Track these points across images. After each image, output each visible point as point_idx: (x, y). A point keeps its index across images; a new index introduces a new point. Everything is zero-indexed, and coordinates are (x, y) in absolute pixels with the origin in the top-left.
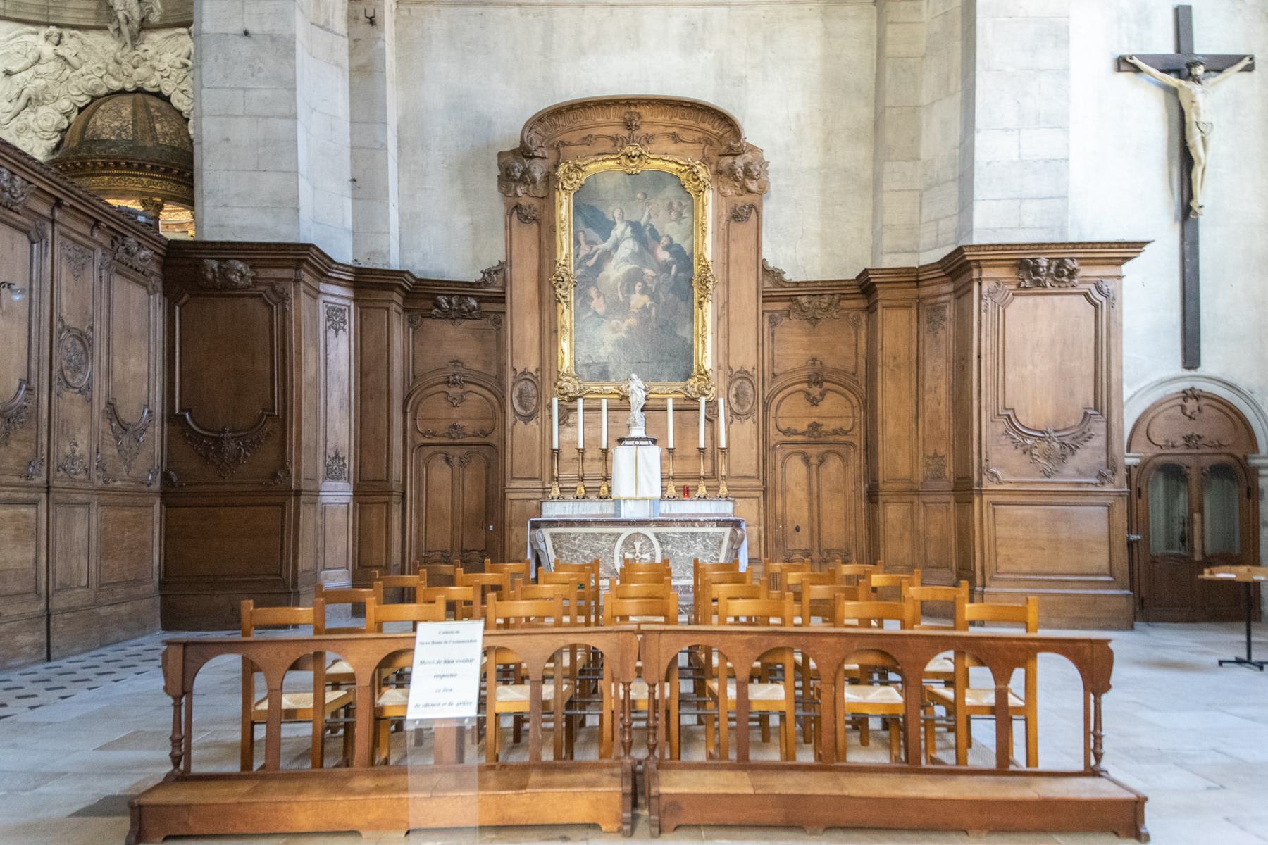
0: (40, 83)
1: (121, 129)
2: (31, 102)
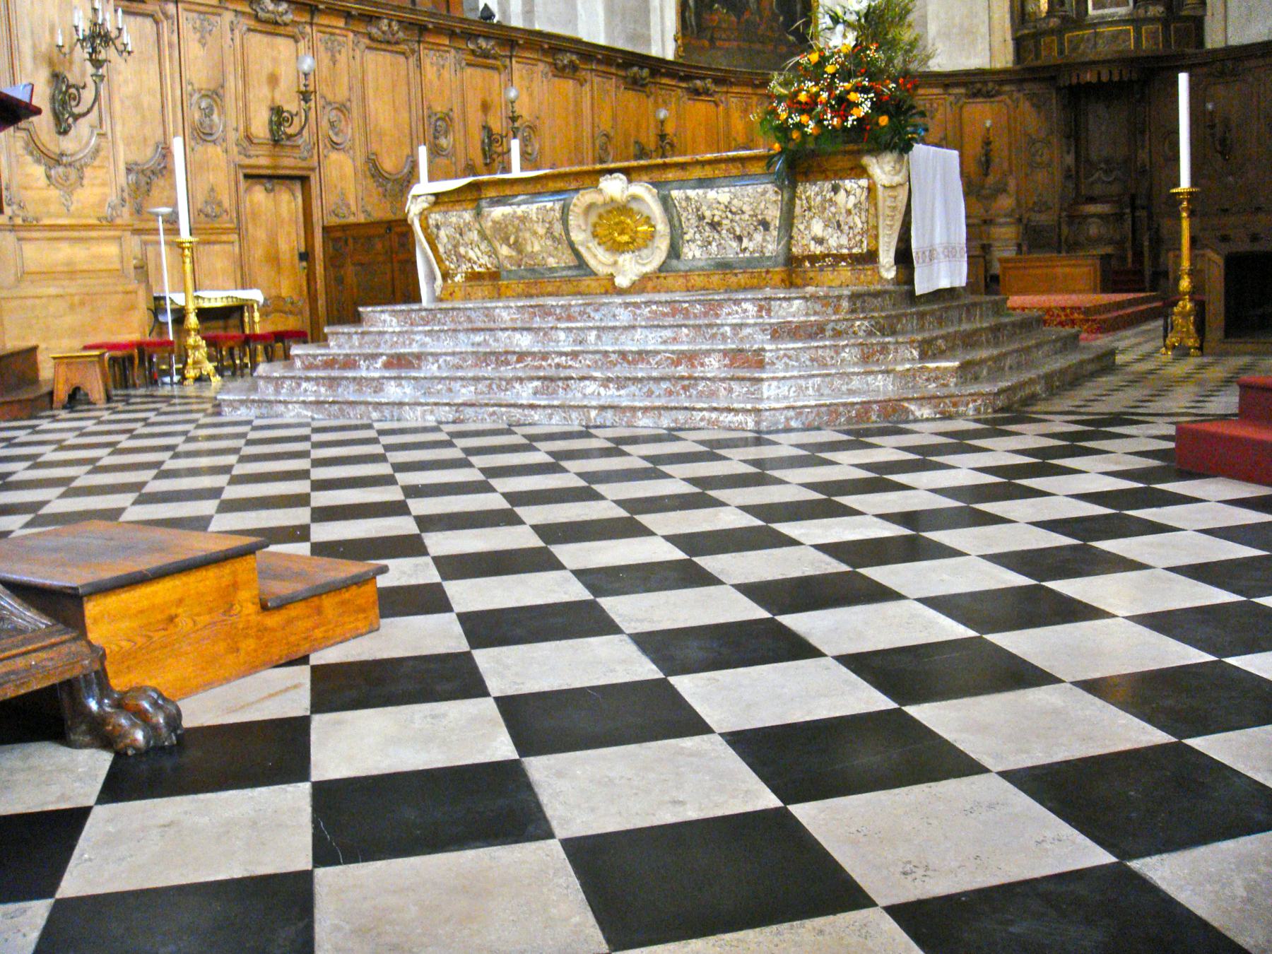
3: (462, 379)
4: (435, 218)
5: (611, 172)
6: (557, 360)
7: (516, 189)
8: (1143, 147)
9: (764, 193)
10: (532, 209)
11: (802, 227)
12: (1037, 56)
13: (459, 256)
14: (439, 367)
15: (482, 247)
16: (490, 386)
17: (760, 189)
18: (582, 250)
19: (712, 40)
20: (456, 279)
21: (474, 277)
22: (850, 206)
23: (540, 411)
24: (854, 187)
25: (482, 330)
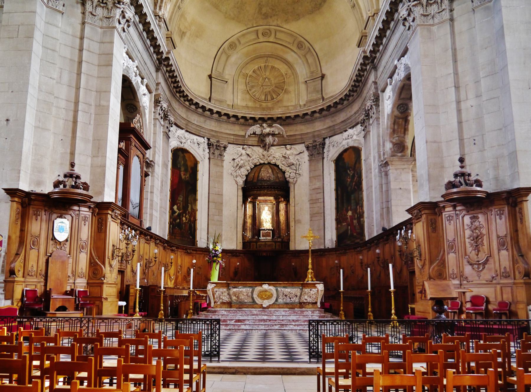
0: (242, 162)
1: (270, 176)
2: (240, 167)
4: (215, 290)
10: (244, 290)
12: (250, 248)
13: (220, 298)
19: (175, 236)
21: (223, 303)
24: (314, 290)
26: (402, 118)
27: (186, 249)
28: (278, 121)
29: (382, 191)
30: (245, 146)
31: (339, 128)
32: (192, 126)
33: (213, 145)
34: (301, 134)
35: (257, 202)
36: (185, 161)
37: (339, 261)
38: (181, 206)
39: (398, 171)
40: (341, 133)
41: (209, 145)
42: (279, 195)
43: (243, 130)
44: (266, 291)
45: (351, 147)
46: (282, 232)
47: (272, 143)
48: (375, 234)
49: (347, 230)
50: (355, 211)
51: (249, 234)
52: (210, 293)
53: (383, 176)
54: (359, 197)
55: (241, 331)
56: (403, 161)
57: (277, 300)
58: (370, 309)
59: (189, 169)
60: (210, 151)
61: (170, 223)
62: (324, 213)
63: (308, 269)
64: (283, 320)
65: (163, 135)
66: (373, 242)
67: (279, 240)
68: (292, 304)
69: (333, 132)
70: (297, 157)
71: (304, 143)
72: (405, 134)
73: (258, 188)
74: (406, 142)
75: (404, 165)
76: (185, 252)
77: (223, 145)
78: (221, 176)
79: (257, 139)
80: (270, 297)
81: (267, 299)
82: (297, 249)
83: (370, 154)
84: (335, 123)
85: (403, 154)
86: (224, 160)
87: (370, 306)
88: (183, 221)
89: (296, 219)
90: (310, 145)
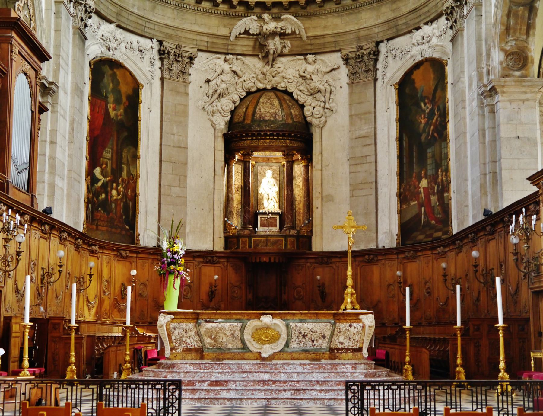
0: (223, 86)
1: (276, 114)
3: (259, 390)
4: (173, 325)
5: (266, 314)
6: (290, 384)
7: (217, 317)
8: (285, 293)
9: (326, 326)
10: (227, 325)
11: (336, 338)
12: (238, 247)
13: (181, 341)
14: (236, 386)
15: (195, 338)
16: (271, 392)
17: (325, 324)
18: (247, 342)
19: (97, 226)
20: (177, 351)
21: (187, 351)
22: (355, 332)
23: (304, 401)
24: (357, 326)
25: (247, 372)
26: (524, 5)
27: (118, 250)
28: (292, 10)
29: (484, 143)
30: (229, 57)
31: (406, 23)
32: (130, 17)
33: (168, 53)
34: (335, 35)
35: (252, 162)
36: (116, 83)
37: (404, 272)
38: (109, 169)
39: (515, 105)
40: (410, 32)
41: (162, 53)
42: (293, 148)
43: (225, 26)
44: (268, 328)
45: (427, 60)
46: (297, 217)
47: (279, 51)
48: (470, 222)
49: (419, 215)
50: (433, 179)
51: (236, 222)
52: (163, 332)
53: (487, 114)
54: (441, 153)
55: (220, 401)
56: (524, 86)
57: (287, 345)
58: (459, 361)
59: (124, 99)
60: (163, 65)
61: (89, 201)
62: (376, 182)
63: (346, 287)
64: (298, 382)
65: (74, 34)
66: (467, 237)
67: (293, 232)
68: (315, 351)
69: (394, 30)
70: (327, 77)
71: (340, 50)
72: (528, 34)
73: (253, 135)
74: (530, 50)
75: (526, 92)
76: (117, 256)
77: (187, 54)
78: (185, 113)
79: (251, 43)
80: (274, 339)
81: (270, 342)
82: (325, 249)
83: (462, 72)
84: (398, 14)
85: (523, 72)
86: (190, 83)
87: (459, 355)
88: (112, 196)
89: (324, 194)
90: (351, 55)
